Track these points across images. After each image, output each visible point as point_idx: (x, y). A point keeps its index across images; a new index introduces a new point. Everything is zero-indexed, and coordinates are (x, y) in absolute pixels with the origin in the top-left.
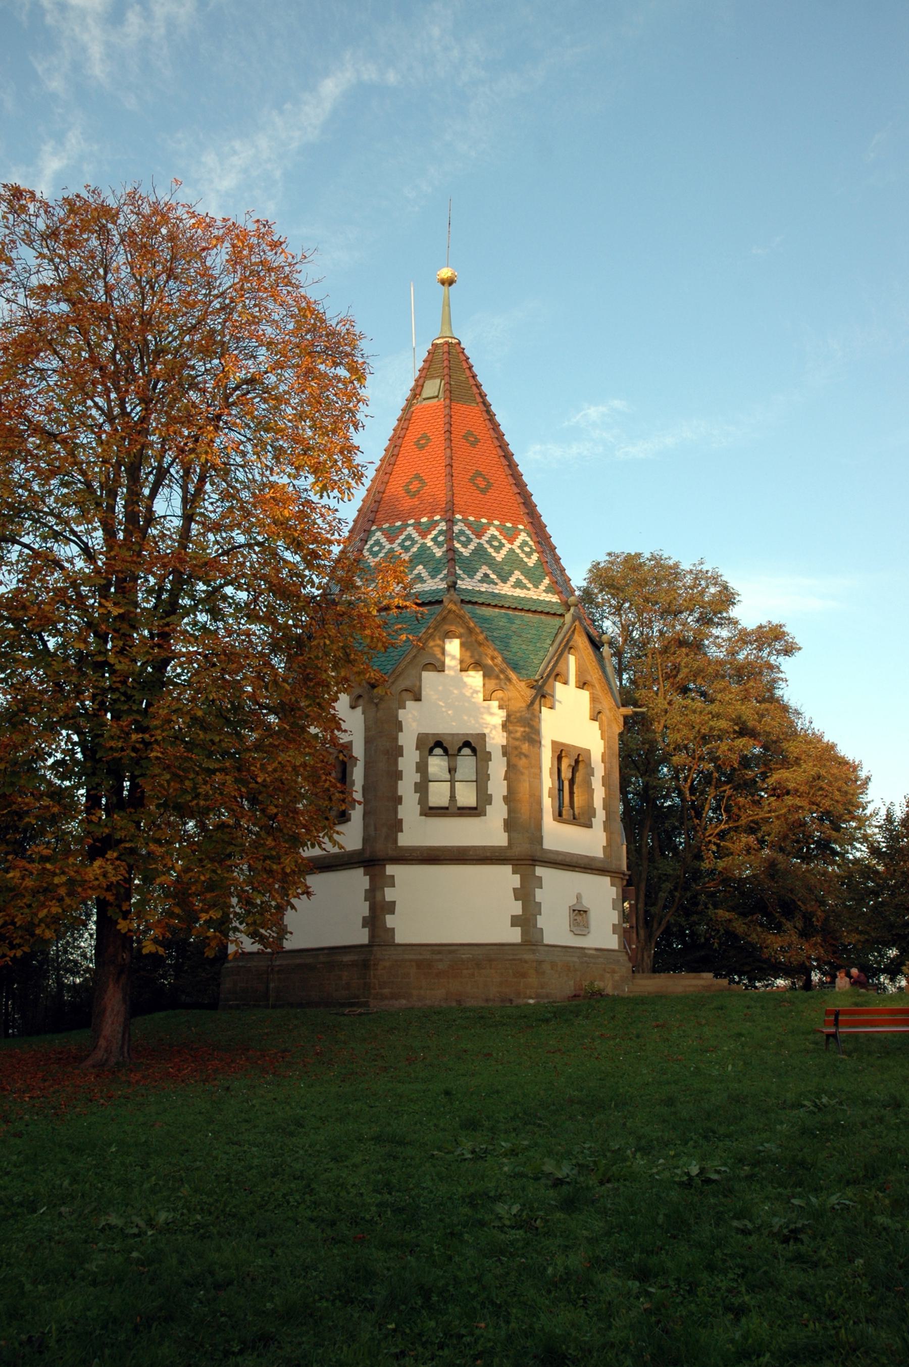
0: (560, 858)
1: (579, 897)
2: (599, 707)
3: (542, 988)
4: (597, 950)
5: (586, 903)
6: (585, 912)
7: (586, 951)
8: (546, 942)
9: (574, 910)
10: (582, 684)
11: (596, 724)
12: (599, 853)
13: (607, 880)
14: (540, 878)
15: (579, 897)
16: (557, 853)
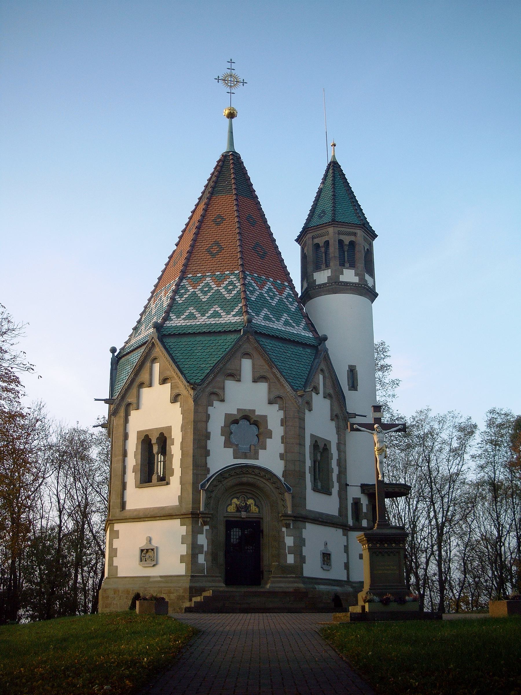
0: (135, 513)
1: (150, 540)
2: (177, 391)
3: (106, 607)
4: (161, 577)
5: (154, 544)
6: (152, 550)
7: (151, 580)
8: (120, 574)
9: (142, 551)
10: (163, 381)
11: (178, 404)
12: (176, 503)
13: (178, 522)
14: (118, 531)
15: (150, 540)
16: (135, 510)
